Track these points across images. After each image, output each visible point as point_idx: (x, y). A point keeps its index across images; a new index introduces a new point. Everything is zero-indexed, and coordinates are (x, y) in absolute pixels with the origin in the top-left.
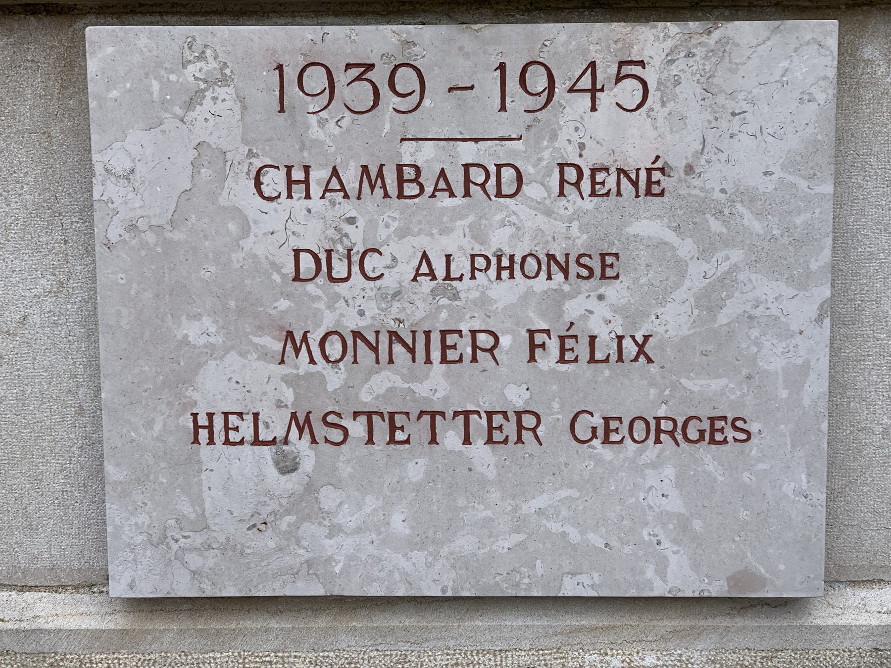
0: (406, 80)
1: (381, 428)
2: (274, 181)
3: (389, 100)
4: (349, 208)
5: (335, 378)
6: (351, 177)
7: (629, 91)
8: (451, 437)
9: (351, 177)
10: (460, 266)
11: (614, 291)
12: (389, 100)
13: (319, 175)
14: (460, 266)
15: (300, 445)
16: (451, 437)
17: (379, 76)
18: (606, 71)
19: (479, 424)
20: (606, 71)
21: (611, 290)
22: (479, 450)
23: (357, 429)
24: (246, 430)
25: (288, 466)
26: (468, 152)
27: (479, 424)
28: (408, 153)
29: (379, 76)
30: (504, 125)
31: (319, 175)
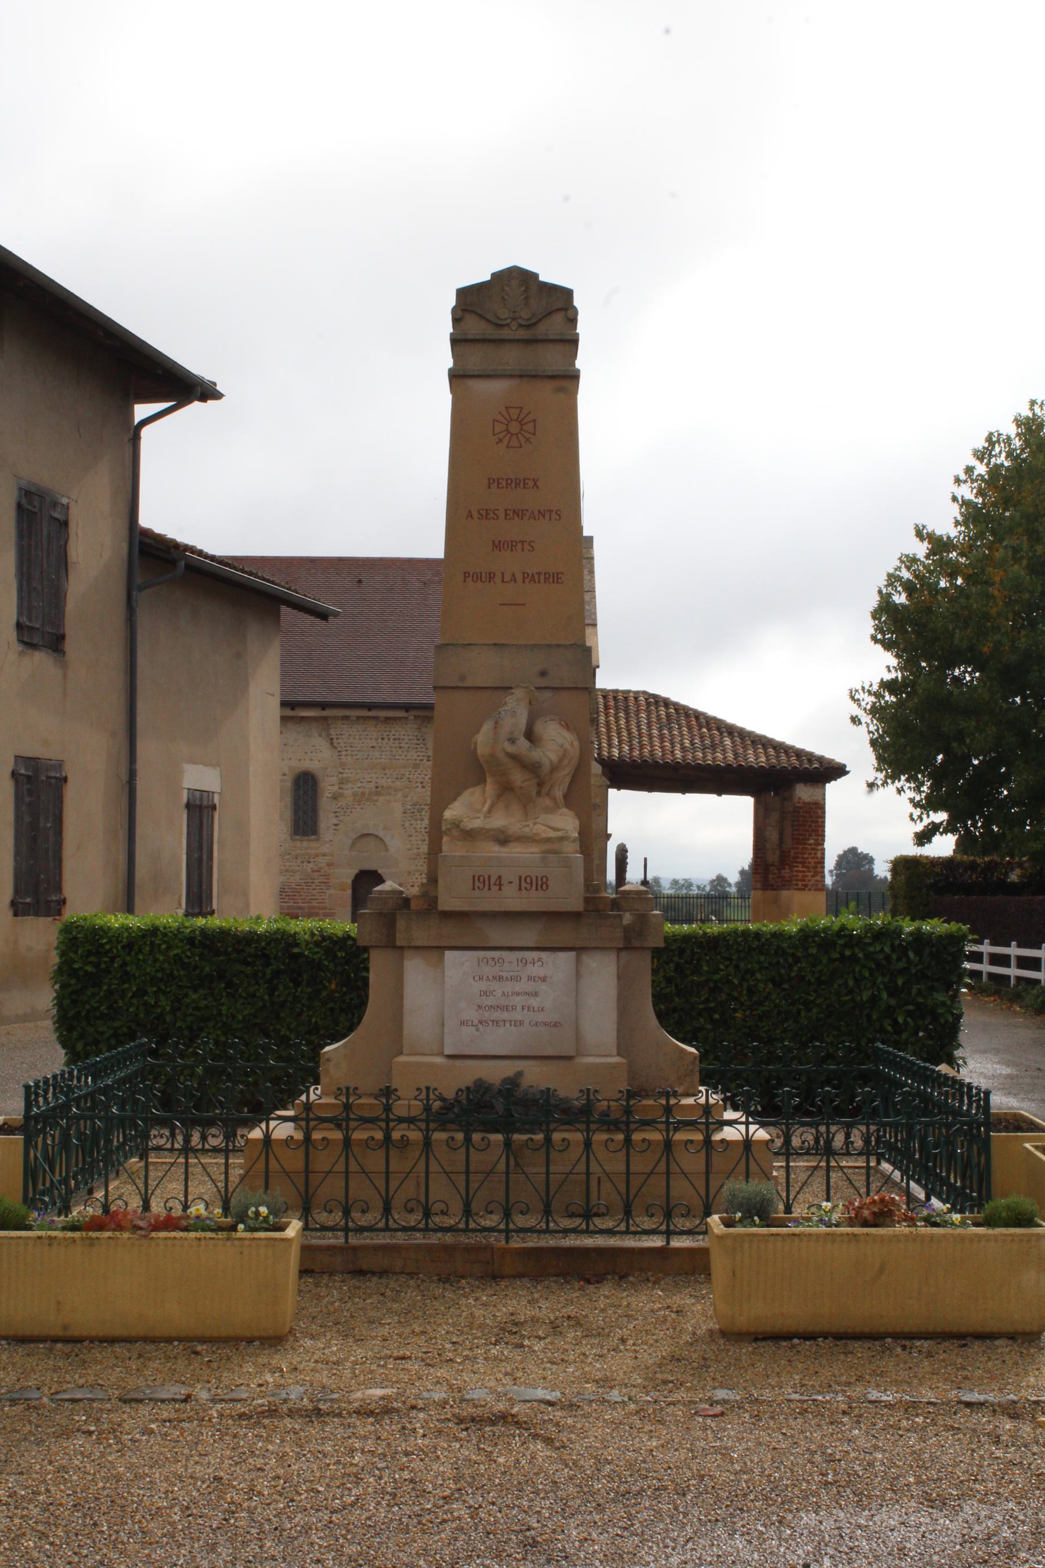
0: (501, 961)
1: (495, 1024)
2: (477, 978)
3: (498, 964)
4: (489, 983)
5: (487, 1014)
6: (491, 978)
7: (540, 963)
8: (508, 1025)
9: (491, 978)
10: (510, 994)
11: (538, 999)
12: (498, 964)
13: (485, 977)
14: (510, 994)
15: (480, 1026)
16: (508, 1025)
17: (496, 960)
18: (536, 960)
19: (513, 1023)
20: (536, 960)
21: (537, 999)
22: (513, 1028)
23: (491, 1023)
24: (470, 1023)
25: (477, 1030)
26: (511, 974)
27: (513, 1023)
28: (501, 974)
29: (496, 960)
30: (518, 969)
31: (485, 977)
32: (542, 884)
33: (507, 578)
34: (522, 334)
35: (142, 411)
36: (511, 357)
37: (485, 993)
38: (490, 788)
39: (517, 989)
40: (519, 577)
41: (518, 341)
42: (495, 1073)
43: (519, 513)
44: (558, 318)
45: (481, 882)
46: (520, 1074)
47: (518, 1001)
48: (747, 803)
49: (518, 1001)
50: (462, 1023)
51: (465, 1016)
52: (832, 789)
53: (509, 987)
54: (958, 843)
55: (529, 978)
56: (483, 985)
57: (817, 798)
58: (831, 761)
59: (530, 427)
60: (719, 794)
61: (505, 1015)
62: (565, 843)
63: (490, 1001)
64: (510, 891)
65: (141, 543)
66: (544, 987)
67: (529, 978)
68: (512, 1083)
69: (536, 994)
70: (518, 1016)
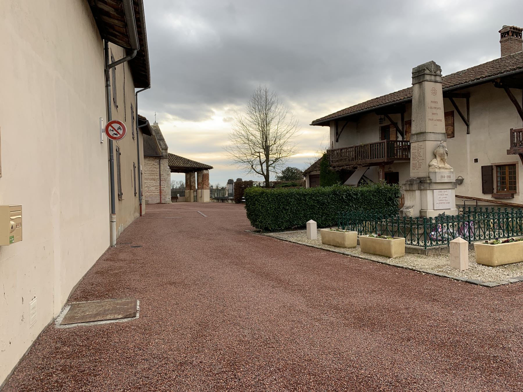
32: (450, 177)
33: (435, 120)
34: (435, 74)
35: (137, 90)
36: (433, 78)
37: (440, 198)
38: (439, 159)
39: (444, 197)
40: (436, 120)
41: (434, 75)
42: (441, 212)
43: (435, 108)
44: (439, 71)
45: (442, 177)
46: (444, 212)
47: (444, 199)
48: (184, 174)
49: (444, 199)
50: (437, 203)
51: (437, 202)
52: (210, 171)
53: (443, 196)
54: (233, 181)
55: (446, 195)
56: (439, 196)
57: (208, 173)
58: (210, 166)
59: (436, 92)
60: (178, 173)
61: (442, 202)
62: (452, 169)
63: (440, 199)
64: (446, 178)
65: (138, 118)
66: (447, 196)
67: (446, 195)
68: (444, 214)
69: (446, 197)
70: (444, 201)
